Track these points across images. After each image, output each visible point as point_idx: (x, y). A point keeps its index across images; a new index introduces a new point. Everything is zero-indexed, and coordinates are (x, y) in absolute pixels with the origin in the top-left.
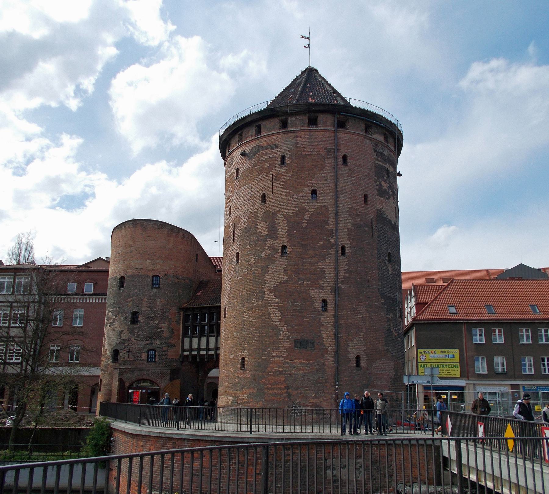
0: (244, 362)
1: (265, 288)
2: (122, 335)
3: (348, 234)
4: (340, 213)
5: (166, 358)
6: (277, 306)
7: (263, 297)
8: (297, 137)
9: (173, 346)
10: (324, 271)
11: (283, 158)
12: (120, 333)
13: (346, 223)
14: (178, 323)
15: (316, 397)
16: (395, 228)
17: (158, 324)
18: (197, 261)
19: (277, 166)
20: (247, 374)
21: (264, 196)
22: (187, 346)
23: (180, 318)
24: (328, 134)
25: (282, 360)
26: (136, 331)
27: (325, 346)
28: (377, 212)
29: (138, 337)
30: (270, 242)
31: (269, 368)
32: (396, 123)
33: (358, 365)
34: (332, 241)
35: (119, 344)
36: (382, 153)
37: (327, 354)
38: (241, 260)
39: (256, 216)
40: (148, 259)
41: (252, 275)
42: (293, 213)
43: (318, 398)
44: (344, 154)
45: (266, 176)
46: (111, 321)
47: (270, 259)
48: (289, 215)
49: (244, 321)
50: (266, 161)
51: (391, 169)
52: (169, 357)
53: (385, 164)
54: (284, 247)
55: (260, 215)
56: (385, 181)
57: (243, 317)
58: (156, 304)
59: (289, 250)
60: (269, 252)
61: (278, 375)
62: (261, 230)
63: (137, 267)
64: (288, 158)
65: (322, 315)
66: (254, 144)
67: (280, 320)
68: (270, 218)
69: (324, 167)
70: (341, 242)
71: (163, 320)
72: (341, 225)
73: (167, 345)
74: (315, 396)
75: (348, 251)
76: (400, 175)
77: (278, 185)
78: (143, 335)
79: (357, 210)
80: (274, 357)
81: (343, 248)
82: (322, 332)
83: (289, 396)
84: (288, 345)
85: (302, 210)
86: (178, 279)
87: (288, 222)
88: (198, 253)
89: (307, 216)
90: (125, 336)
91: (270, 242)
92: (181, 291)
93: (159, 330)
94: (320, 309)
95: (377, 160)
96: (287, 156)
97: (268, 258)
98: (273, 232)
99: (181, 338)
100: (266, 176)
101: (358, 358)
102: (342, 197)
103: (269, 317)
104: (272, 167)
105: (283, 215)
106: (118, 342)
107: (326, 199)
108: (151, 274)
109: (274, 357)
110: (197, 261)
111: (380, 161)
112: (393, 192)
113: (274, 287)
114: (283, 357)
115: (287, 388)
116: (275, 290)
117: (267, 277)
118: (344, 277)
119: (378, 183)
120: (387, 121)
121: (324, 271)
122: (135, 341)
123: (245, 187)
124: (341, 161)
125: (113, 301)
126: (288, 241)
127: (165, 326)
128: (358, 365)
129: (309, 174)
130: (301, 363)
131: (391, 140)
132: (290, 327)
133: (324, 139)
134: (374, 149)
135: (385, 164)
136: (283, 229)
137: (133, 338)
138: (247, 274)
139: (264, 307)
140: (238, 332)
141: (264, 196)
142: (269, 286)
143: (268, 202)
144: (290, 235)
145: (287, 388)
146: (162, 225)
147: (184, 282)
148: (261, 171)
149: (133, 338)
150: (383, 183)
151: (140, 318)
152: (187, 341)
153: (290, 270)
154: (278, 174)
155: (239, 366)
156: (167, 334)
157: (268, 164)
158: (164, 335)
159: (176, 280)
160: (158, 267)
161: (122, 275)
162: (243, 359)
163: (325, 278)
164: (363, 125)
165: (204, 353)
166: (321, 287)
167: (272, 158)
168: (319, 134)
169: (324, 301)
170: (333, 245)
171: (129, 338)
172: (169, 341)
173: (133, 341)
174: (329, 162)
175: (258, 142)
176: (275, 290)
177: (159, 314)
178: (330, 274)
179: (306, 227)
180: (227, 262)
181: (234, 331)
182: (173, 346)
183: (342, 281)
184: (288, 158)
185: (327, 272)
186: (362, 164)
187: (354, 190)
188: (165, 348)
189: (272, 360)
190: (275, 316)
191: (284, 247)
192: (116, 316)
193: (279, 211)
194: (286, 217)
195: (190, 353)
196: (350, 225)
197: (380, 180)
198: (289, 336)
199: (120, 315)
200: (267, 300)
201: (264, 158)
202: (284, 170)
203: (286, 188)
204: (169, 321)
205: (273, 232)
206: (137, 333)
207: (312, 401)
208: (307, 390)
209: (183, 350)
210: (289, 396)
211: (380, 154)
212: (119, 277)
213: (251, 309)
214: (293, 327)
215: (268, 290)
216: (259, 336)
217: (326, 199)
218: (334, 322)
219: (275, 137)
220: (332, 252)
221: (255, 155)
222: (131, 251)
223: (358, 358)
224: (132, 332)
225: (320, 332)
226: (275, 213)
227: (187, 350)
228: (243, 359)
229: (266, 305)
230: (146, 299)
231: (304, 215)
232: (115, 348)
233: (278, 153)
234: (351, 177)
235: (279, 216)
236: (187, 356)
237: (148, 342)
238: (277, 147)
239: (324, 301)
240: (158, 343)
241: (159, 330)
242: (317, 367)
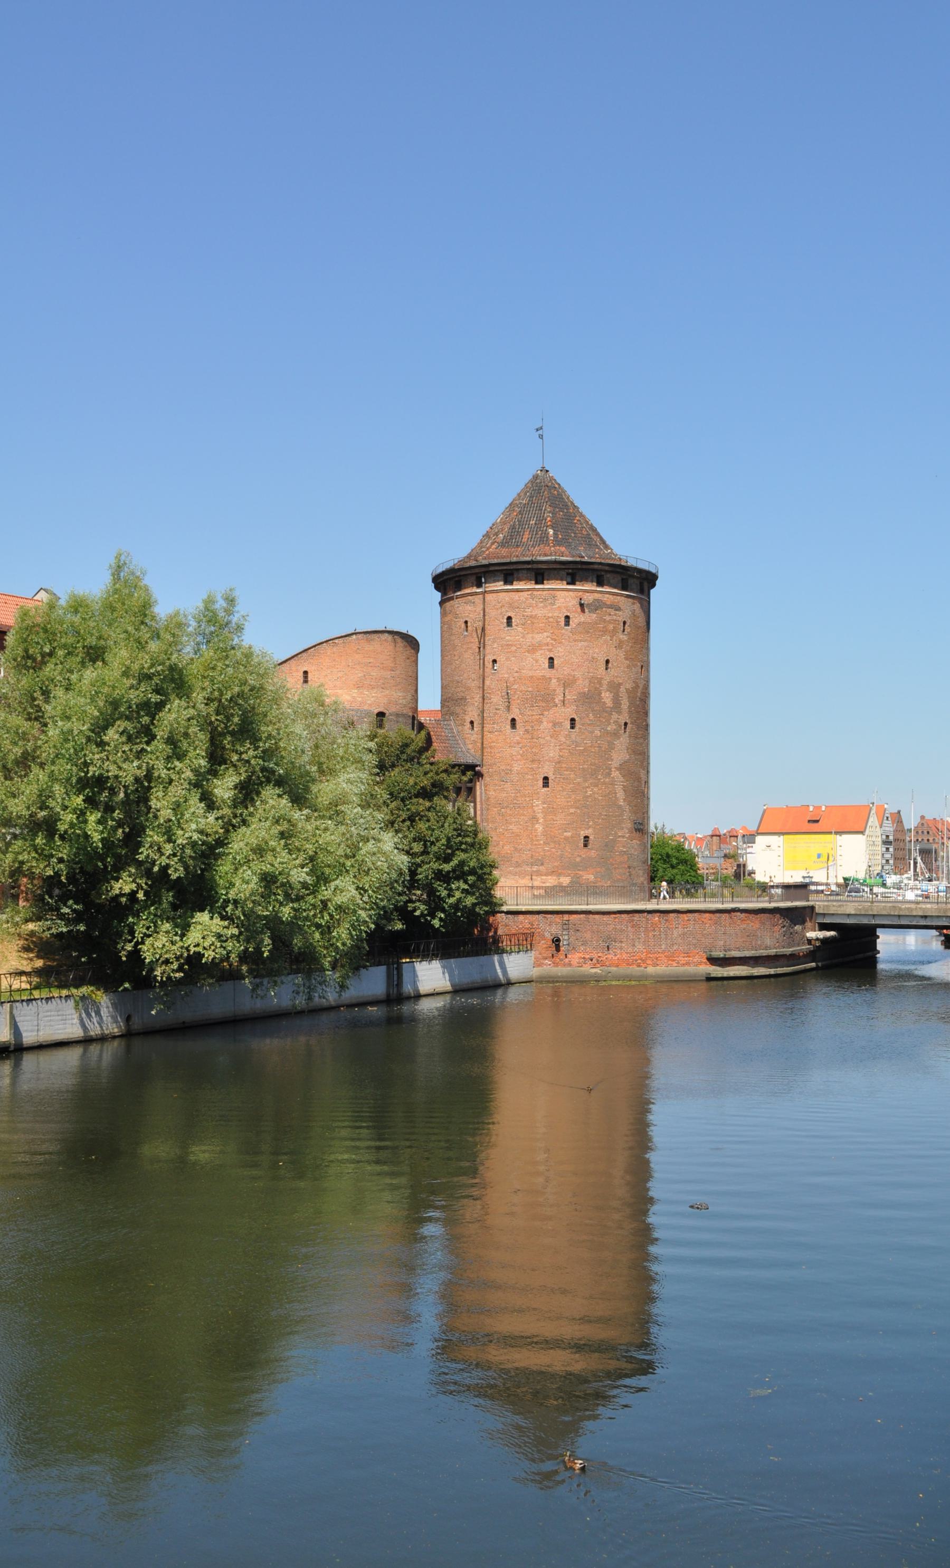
7: (609, 774)
20: (593, 853)
21: (607, 662)
30: (615, 716)
39: (600, 681)
47: (616, 735)
49: (588, 797)
50: (609, 622)
54: (626, 724)
59: (629, 726)
60: (614, 727)
66: (597, 596)
68: (614, 687)
77: (622, 655)
91: (615, 716)
104: (615, 631)
115: (629, 867)
116: (620, 769)
117: (614, 755)
123: (585, 644)
140: (577, 808)
141: (607, 662)
142: (615, 763)
145: (629, 867)
148: (605, 631)
154: (621, 642)
157: (611, 627)
175: (600, 595)
176: (620, 769)
181: (571, 807)
190: (621, 795)
201: (608, 618)
212: (376, 711)
213: (597, 786)
226: (620, 684)
228: (586, 837)
229: (613, 783)
235: (622, 689)
238: (619, 609)
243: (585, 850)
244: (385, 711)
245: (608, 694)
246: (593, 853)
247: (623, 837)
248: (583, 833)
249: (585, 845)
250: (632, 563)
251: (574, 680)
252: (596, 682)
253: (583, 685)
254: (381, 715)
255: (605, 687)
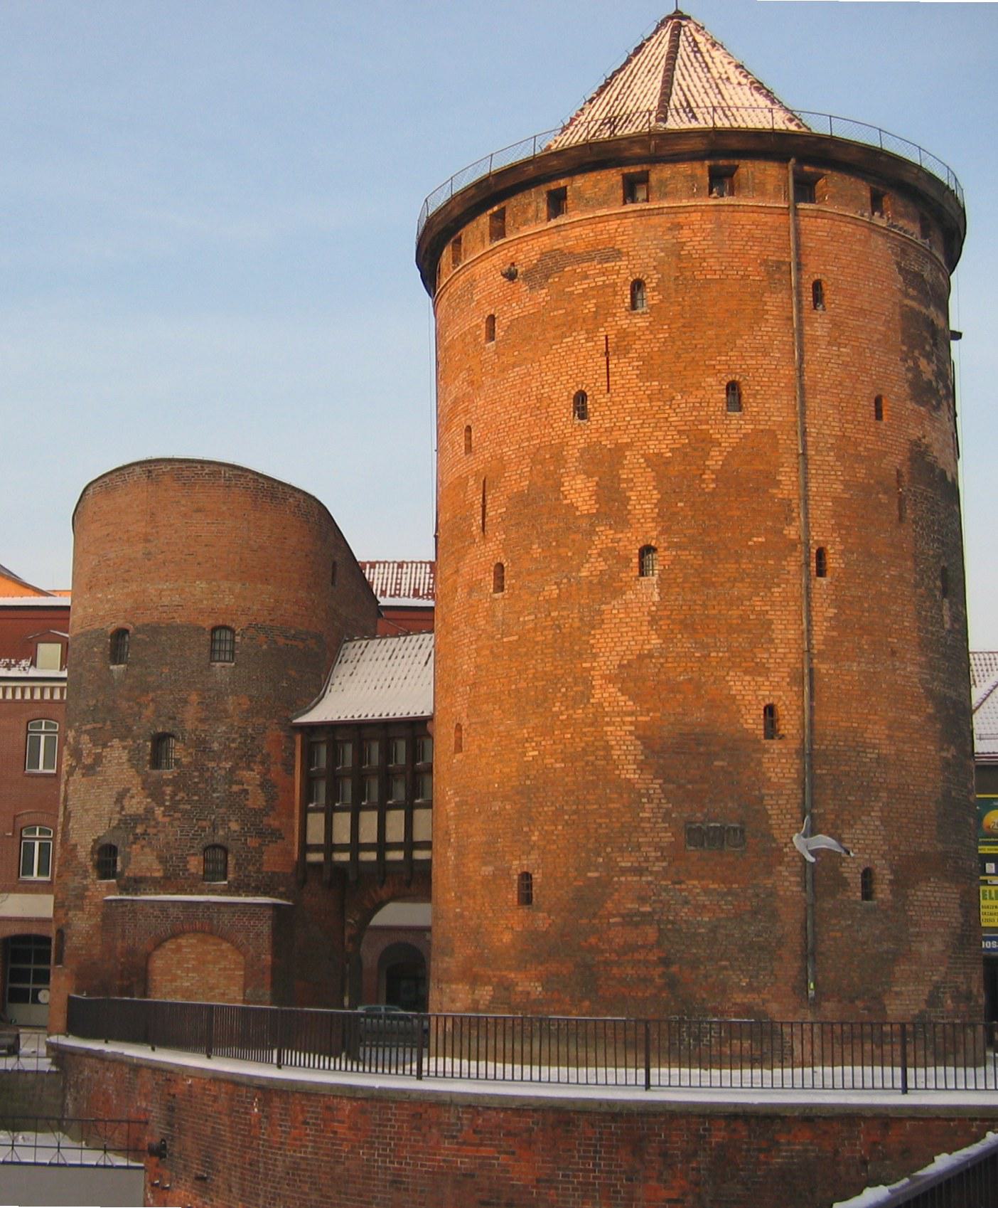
0: (529, 887)
1: (593, 668)
2: (126, 803)
3: (835, 515)
4: (811, 452)
5: (259, 871)
6: (631, 723)
7: (586, 696)
8: (679, 226)
9: (276, 835)
10: (771, 622)
11: (638, 285)
12: (120, 798)
13: (828, 483)
14: (289, 768)
15: (750, 988)
16: (951, 492)
17: (232, 771)
18: (333, 583)
19: (621, 312)
21: (581, 398)
22: (316, 833)
23: (293, 755)
24: (764, 218)
25: (649, 883)
26: (168, 790)
27: (774, 840)
28: (911, 451)
29: (174, 807)
31: (609, 905)
32: (952, 187)
33: (867, 894)
34: (792, 532)
35: (117, 827)
36: (918, 275)
37: (780, 863)
38: (512, 587)
39: (559, 459)
40: (199, 577)
41: (549, 634)
42: (672, 450)
43: (758, 990)
44: (816, 277)
45: (587, 340)
46: (88, 761)
48: (660, 455)
51: (940, 322)
52: (265, 869)
53: (927, 307)
55: (572, 453)
56: (928, 356)
57: (524, 754)
58: (225, 711)
61: (636, 925)
62: (574, 498)
63: (166, 601)
64: (654, 289)
65: (767, 751)
67: (642, 766)
68: (605, 464)
69: (759, 315)
70: (816, 537)
71: (246, 757)
72: (813, 486)
73: (260, 834)
74: (750, 984)
75: (833, 562)
76: (958, 336)
78: (188, 802)
79: (856, 444)
80: (624, 871)
81: (821, 554)
82: (768, 802)
83: (672, 984)
84: (667, 837)
85: (701, 442)
86: (287, 637)
87: (660, 478)
88: (337, 558)
89: (715, 460)
90: (136, 805)
91: (604, 535)
92: (293, 673)
93: (235, 788)
94: (760, 731)
95: (906, 295)
96: (651, 284)
97: (600, 583)
98: (612, 503)
99: (297, 811)
100: (587, 340)
101: (867, 875)
102: (813, 403)
103: (608, 757)
104: (602, 313)
105: (643, 456)
106: (114, 823)
107: (770, 407)
108: (208, 623)
109: (624, 871)
110: (333, 583)
111: (913, 298)
112: (946, 387)
113: (619, 666)
114: (651, 873)
117: (599, 639)
118: (828, 641)
119: (910, 363)
120: (932, 178)
121: (771, 622)
122: (167, 819)
124: (808, 298)
125: (92, 702)
126: (661, 533)
127: (251, 776)
128: (867, 894)
129: (717, 336)
130: (706, 891)
131: (937, 235)
132: (671, 786)
133: (757, 233)
134: (898, 264)
135: (927, 307)
136: (643, 499)
137: (159, 811)
138: (535, 630)
139: (592, 725)
141: (581, 398)
143: (595, 417)
144: (666, 516)
145: (666, 962)
146: (235, 476)
147: (301, 645)
148: (570, 324)
149: (159, 811)
150: (923, 362)
151: (178, 751)
152: (316, 823)
153: (668, 617)
154: (623, 334)
155: (513, 896)
156: (257, 800)
157: (591, 305)
158: (250, 804)
159: (281, 641)
160: (229, 600)
161: (120, 623)
162: (526, 877)
163: (771, 641)
164: (866, 194)
165: (372, 856)
166: (760, 670)
167: (605, 286)
168: (743, 218)
169: (770, 710)
170: (793, 545)
171: (149, 811)
172: (265, 820)
173: (160, 819)
174: (774, 302)
175: (556, 238)
177: (234, 740)
178: (785, 631)
179: (713, 494)
180: (461, 594)
182: (276, 835)
183: (821, 653)
184: (654, 289)
185: (778, 626)
186: (866, 306)
187: (847, 383)
188: (253, 842)
189: (619, 883)
191: (647, 550)
192: (105, 746)
193: (629, 446)
194: (655, 462)
195: (328, 857)
196: (839, 487)
197: (916, 353)
198: (667, 815)
199: (116, 742)
200: (600, 704)
201: (579, 288)
202: (641, 322)
203: (650, 377)
204: (263, 763)
205: (612, 503)
206: (172, 798)
207: (739, 998)
208: (725, 968)
209: (305, 848)
210: (672, 984)
211: (913, 278)
212: (111, 629)
214: (680, 787)
215: (603, 677)
216: (575, 812)
217: (770, 407)
218: (801, 772)
219: (613, 225)
220: (792, 565)
221: (547, 277)
222: (148, 555)
223: (867, 875)
224: (153, 789)
225: (761, 799)
226: (620, 449)
227: (317, 848)
230: (194, 698)
231: (707, 455)
232: (106, 841)
233: (623, 272)
234: (839, 345)
235: (632, 458)
236: (317, 866)
237: (204, 823)
238: (618, 254)
239: (770, 710)
240: (234, 826)
241: (235, 788)
242: (754, 900)
243: (522, 912)
244: (128, 626)
245: (579, 482)
246: (542, 921)
247: (639, 871)
248: (517, 866)
249: (526, 897)
250: (842, 131)
251: (501, 464)
252: (549, 460)
253: (517, 479)
254: (120, 634)
255: (572, 465)
